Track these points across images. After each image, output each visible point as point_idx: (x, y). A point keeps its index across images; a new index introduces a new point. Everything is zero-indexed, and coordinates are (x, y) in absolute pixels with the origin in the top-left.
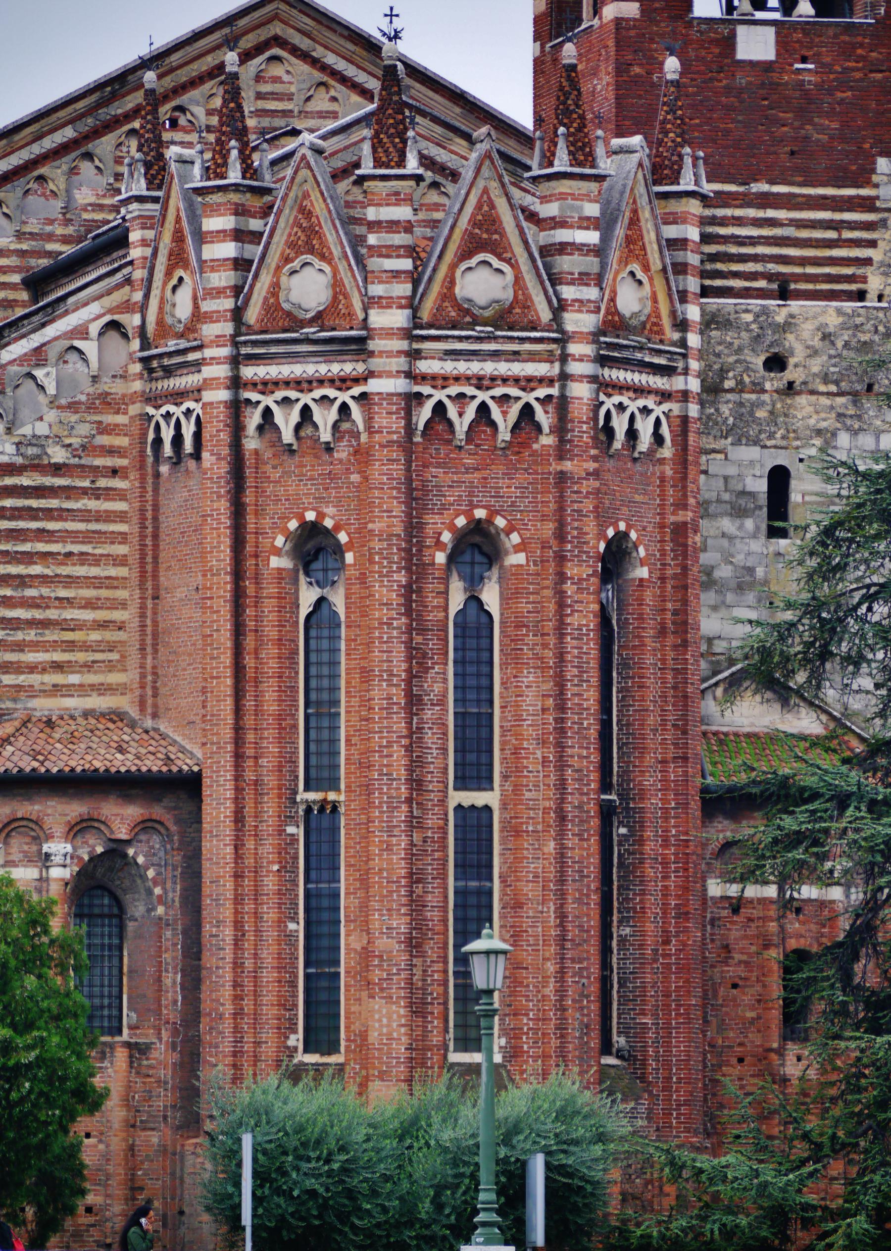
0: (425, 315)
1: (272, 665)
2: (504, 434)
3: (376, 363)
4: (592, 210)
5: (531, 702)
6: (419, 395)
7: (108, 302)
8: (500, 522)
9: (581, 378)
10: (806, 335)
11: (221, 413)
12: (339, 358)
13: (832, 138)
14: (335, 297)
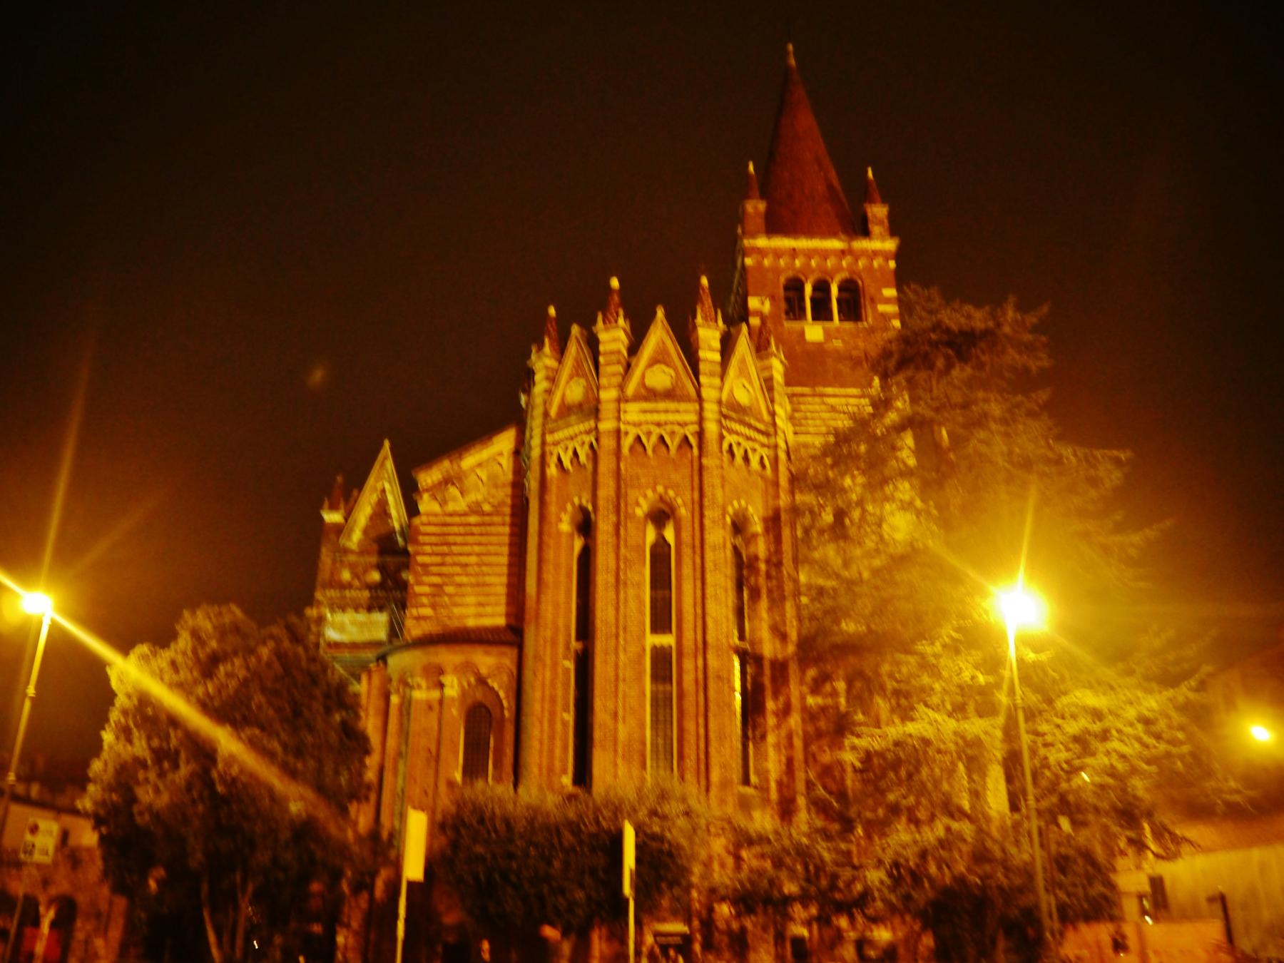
8: (671, 493)
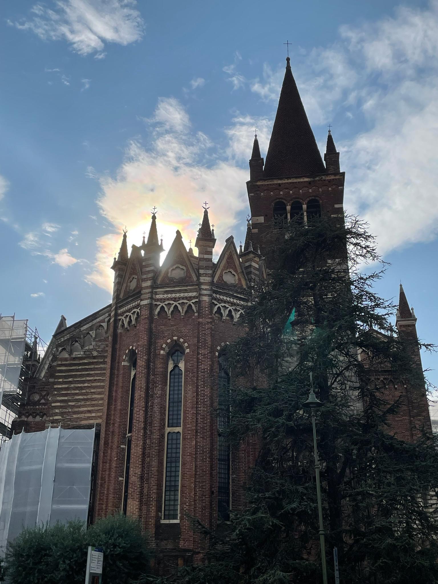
1: (120, 395)
5: (190, 394)
8: (182, 340)
9: (205, 295)
14: (137, 284)
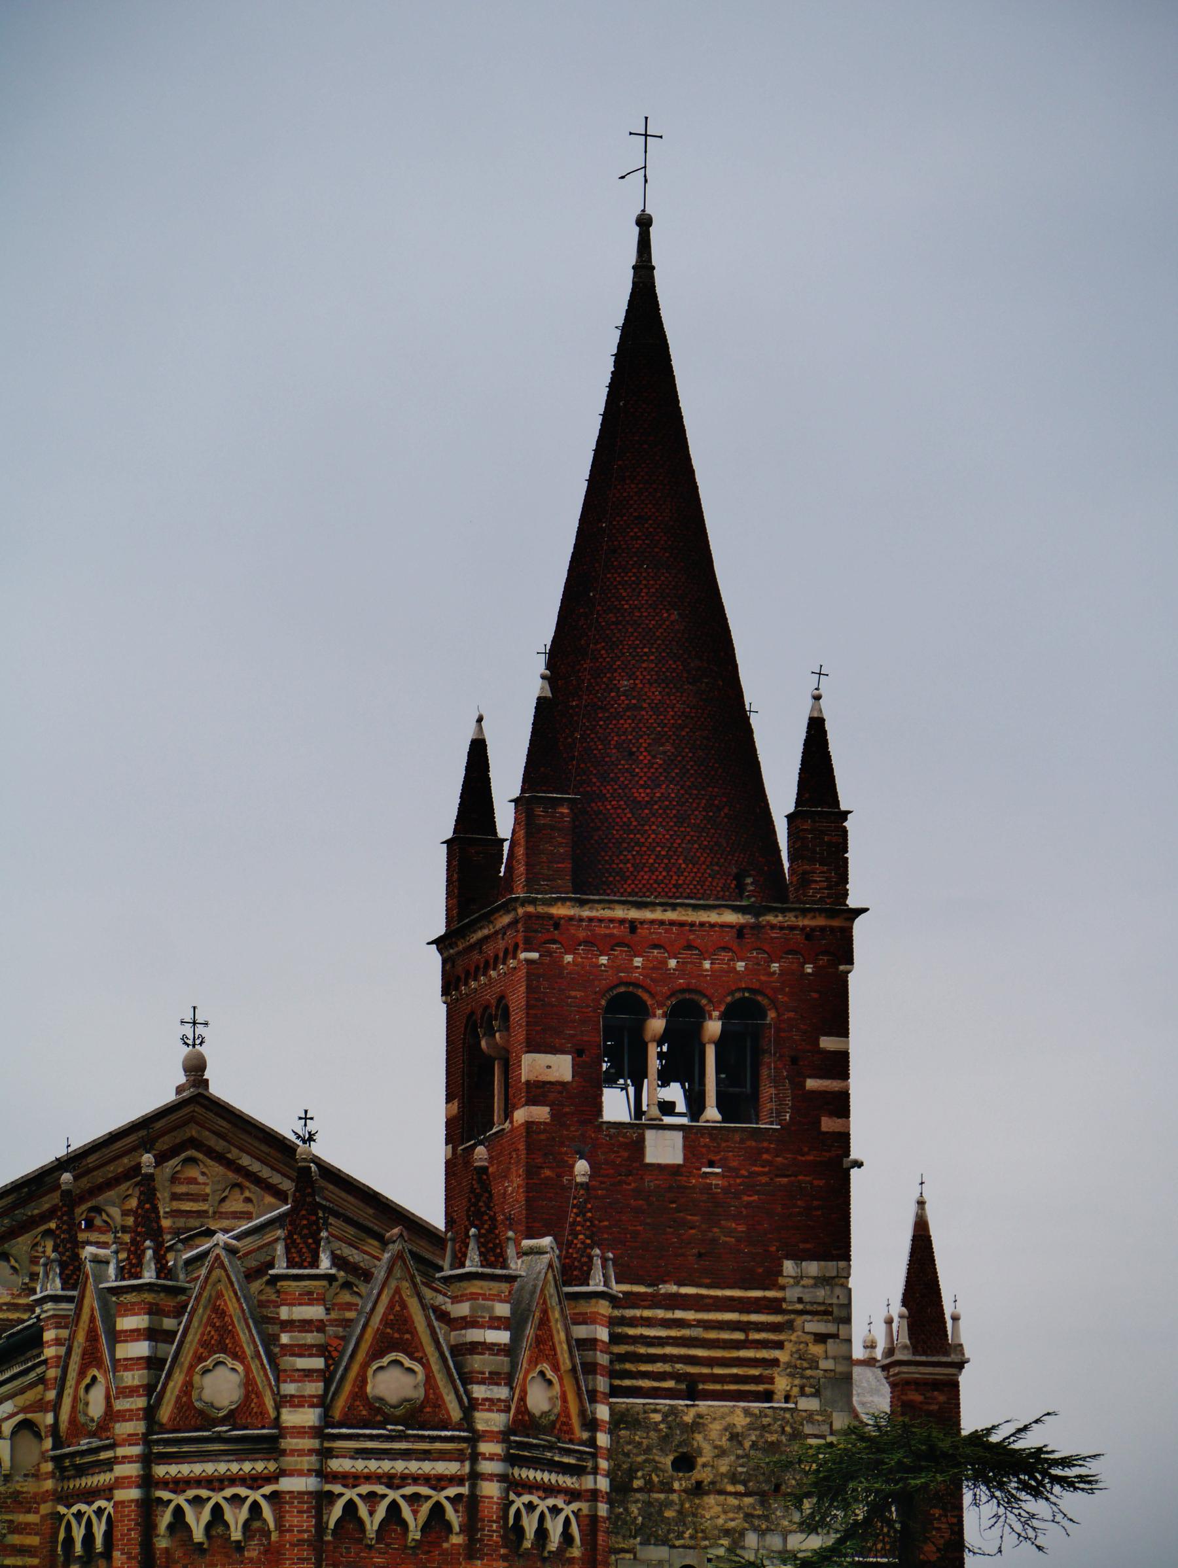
0: (337, 1414)
2: (415, 1534)
3: (289, 1462)
4: (503, 1310)
6: (330, 1493)
7: (21, 1400)
9: (490, 1477)
10: (714, 1435)
11: (132, 1512)
12: (250, 1456)
13: (738, 1240)
14: (247, 1398)
